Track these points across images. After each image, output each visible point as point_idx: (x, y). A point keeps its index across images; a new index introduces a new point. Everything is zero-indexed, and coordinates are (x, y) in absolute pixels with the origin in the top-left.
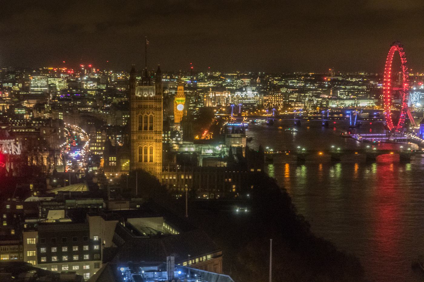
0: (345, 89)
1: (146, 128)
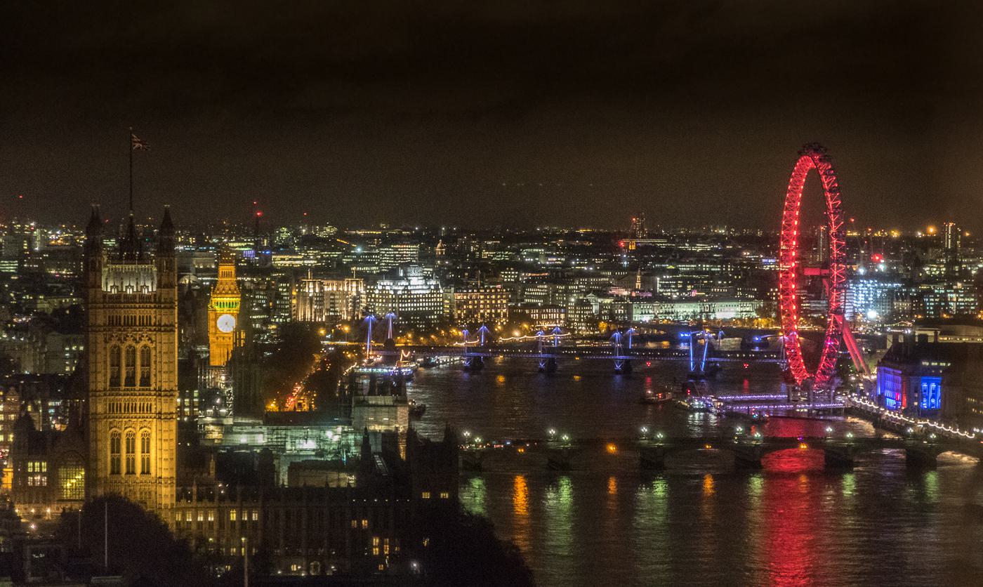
0: (676, 271)
1: (130, 381)
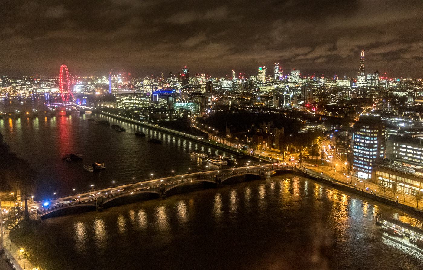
0: (45, 84)
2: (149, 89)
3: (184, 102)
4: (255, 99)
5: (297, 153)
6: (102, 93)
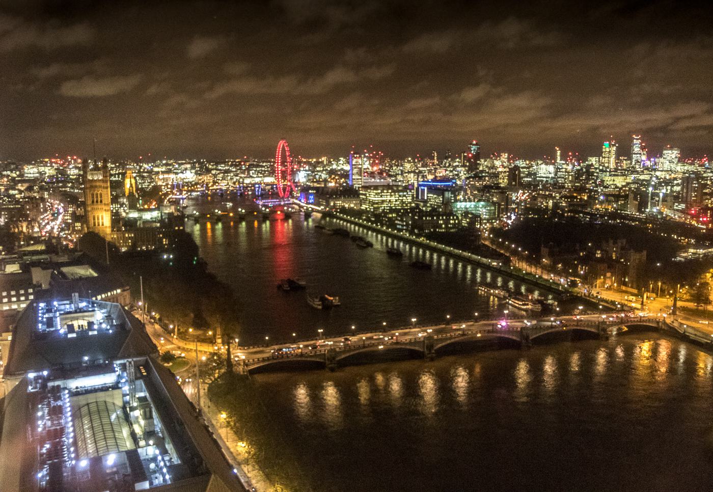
1: (97, 202)
2: (412, 178)
3: (470, 201)
4: (596, 199)
5: (668, 297)
6: (337, 185)
